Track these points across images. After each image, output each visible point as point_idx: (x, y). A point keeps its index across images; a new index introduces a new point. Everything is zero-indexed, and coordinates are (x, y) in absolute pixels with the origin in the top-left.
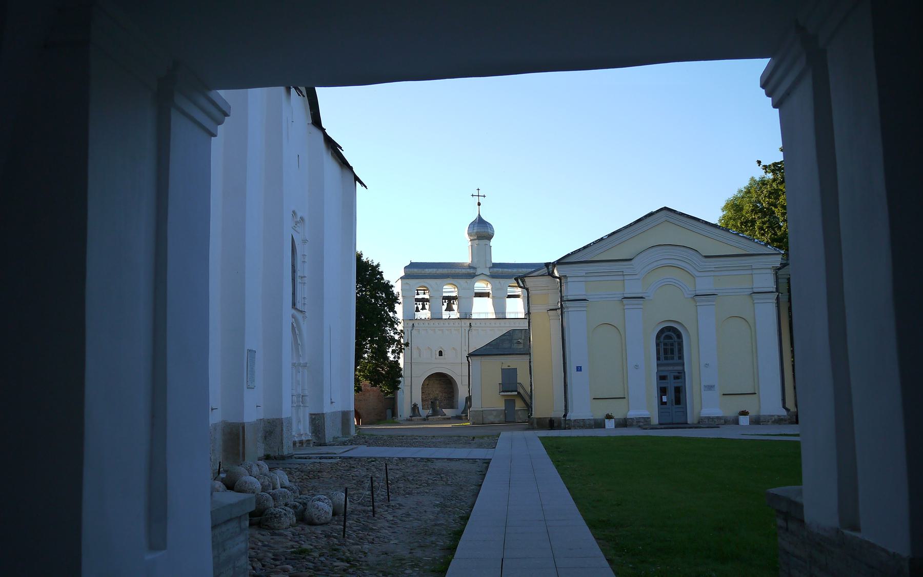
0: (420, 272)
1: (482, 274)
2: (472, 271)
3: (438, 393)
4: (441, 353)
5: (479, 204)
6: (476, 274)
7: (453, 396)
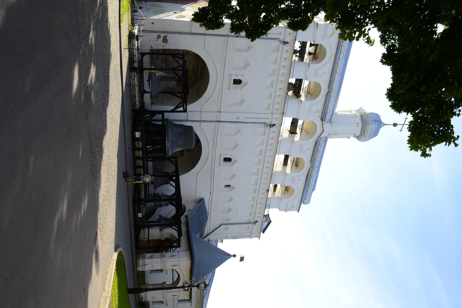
0: (342, 52)
2: (328, 117)
4: (237, 82)
5: (395, 125)
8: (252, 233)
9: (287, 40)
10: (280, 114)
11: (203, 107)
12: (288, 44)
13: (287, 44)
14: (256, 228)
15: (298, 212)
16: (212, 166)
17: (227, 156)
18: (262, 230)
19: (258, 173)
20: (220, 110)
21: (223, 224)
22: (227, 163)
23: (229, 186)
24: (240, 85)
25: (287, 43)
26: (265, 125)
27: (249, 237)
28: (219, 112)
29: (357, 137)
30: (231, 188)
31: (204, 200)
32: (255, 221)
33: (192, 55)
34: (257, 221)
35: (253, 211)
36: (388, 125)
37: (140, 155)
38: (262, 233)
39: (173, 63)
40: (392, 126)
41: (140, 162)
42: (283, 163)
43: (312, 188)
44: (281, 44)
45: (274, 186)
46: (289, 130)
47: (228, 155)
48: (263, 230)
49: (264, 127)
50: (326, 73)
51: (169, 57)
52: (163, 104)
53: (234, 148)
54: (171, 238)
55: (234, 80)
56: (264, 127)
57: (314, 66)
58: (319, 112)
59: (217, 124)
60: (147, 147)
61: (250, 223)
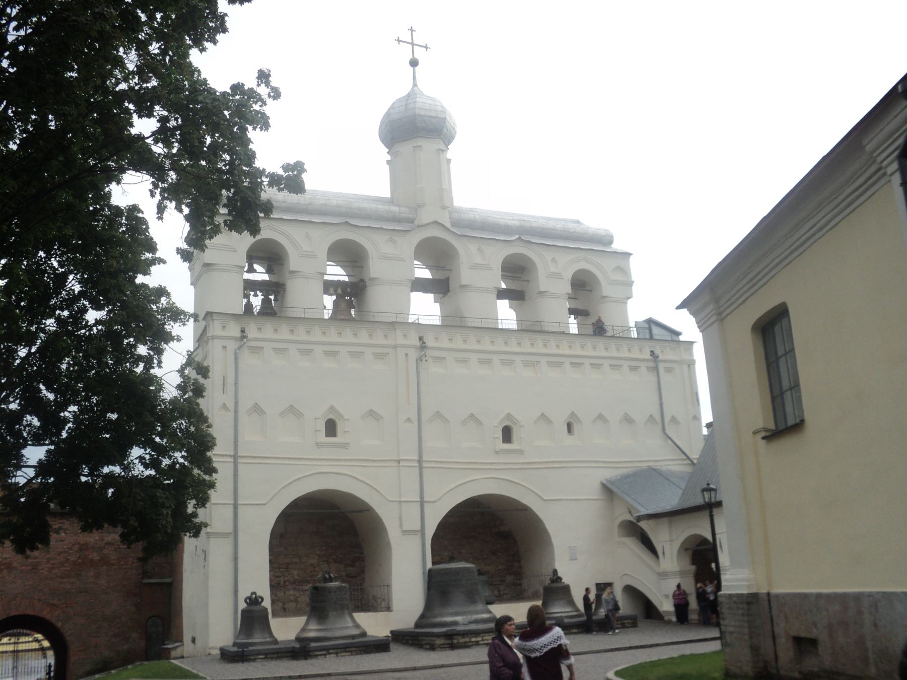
1: (436, 223)
2: (404, 212)
3: (314, 561)
4: (331, 428)
5: (414, 63)
6: (417, 222)
7: (363, 571)
8: (680, 362)
9: (238, 334)
10: (395, 329)
11: (390, 499)
12: (244, 328)
13: (246, 332)
14: (668, 354)
15: (632, 254)
17: (498, 438)
18: (675, 338)
19: (534, 364)
20: (394, 460)
21: (664, 429)
22: (515, 436)
23: (570, 427)
24: (337, 421)
25: (243, 331)
26: (421, 360)
27: (691, 366)
28: (399, 463)
29: (447, 143)
30: (573, 421)
31: (608, 481)
32: (651, 357)
34: (651, 352)
35: (626, 364)
36: (414, 78)
38: (682, 338)
40: (417, 68)
42: (520, 302)
43: (576, 225)
44: (246, 345)
45: (576, 316)
46: (442, 295)
47: (497, 436)
48: (673, 335)
49: (426, 361)
50: (307, 233)
51: (291, 577)
52: (389, 586)
53: (479, 423)
54: (690, 552)
55: (328, 435)
56: (426, 361)
57: (294, 262)
58: (393, 237)
59: (425, 465)
61: (656, 369)
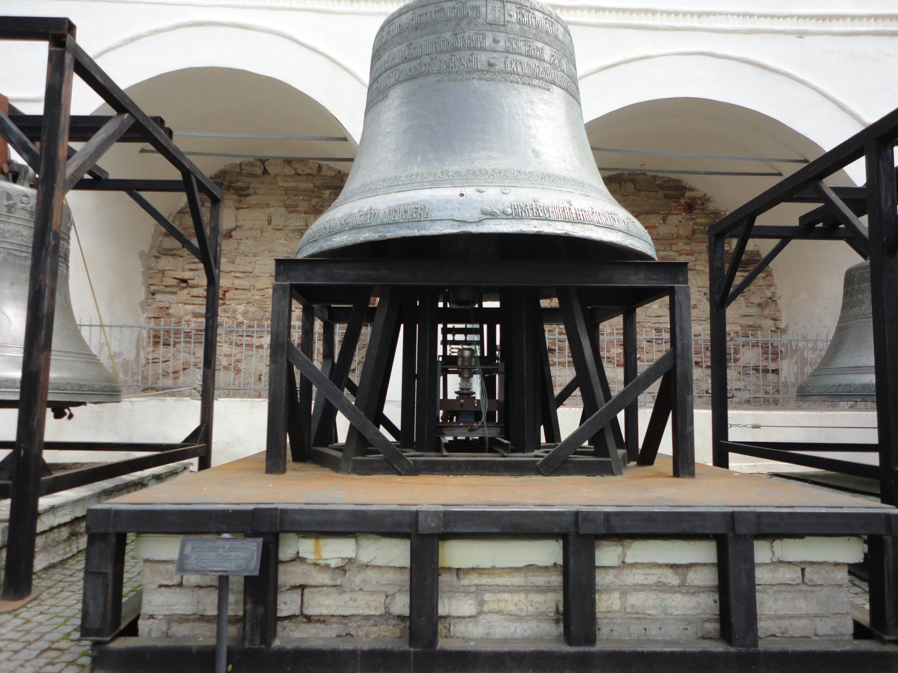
16: (801, 34)
33: (236, 217)
37: (530, 568)
39: (257, 297)
41: (655, 576)
60: (13, 507)
